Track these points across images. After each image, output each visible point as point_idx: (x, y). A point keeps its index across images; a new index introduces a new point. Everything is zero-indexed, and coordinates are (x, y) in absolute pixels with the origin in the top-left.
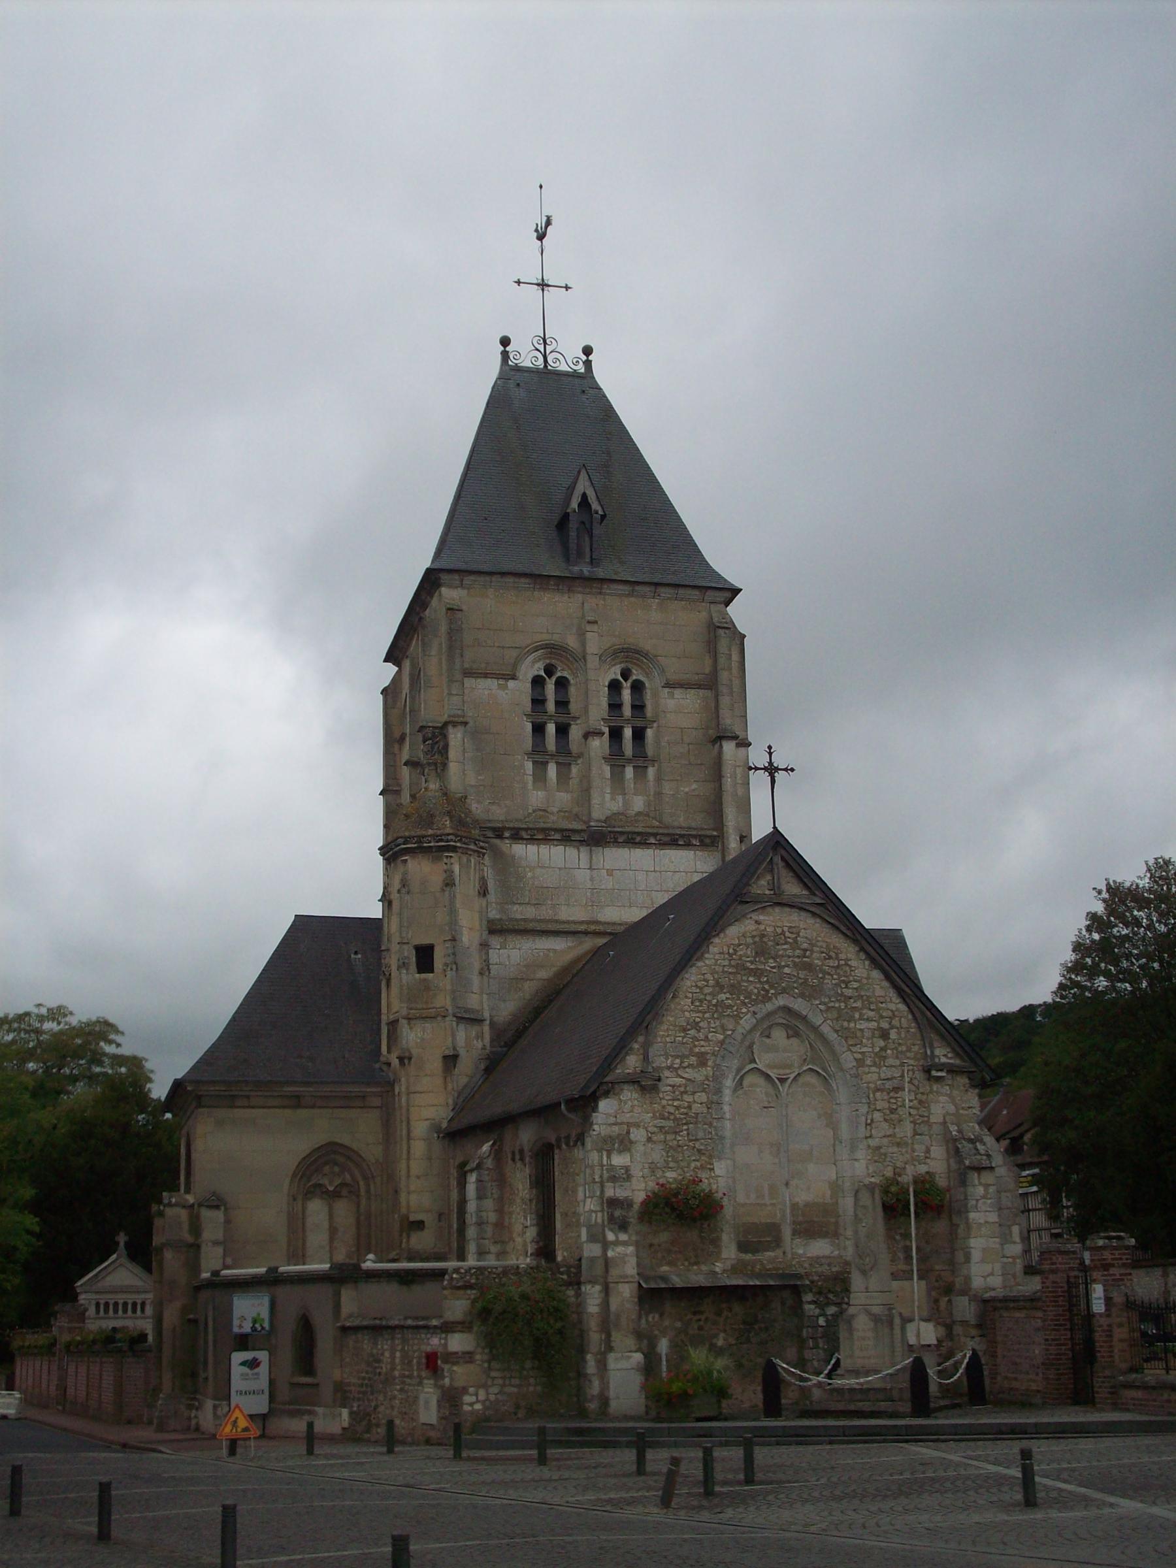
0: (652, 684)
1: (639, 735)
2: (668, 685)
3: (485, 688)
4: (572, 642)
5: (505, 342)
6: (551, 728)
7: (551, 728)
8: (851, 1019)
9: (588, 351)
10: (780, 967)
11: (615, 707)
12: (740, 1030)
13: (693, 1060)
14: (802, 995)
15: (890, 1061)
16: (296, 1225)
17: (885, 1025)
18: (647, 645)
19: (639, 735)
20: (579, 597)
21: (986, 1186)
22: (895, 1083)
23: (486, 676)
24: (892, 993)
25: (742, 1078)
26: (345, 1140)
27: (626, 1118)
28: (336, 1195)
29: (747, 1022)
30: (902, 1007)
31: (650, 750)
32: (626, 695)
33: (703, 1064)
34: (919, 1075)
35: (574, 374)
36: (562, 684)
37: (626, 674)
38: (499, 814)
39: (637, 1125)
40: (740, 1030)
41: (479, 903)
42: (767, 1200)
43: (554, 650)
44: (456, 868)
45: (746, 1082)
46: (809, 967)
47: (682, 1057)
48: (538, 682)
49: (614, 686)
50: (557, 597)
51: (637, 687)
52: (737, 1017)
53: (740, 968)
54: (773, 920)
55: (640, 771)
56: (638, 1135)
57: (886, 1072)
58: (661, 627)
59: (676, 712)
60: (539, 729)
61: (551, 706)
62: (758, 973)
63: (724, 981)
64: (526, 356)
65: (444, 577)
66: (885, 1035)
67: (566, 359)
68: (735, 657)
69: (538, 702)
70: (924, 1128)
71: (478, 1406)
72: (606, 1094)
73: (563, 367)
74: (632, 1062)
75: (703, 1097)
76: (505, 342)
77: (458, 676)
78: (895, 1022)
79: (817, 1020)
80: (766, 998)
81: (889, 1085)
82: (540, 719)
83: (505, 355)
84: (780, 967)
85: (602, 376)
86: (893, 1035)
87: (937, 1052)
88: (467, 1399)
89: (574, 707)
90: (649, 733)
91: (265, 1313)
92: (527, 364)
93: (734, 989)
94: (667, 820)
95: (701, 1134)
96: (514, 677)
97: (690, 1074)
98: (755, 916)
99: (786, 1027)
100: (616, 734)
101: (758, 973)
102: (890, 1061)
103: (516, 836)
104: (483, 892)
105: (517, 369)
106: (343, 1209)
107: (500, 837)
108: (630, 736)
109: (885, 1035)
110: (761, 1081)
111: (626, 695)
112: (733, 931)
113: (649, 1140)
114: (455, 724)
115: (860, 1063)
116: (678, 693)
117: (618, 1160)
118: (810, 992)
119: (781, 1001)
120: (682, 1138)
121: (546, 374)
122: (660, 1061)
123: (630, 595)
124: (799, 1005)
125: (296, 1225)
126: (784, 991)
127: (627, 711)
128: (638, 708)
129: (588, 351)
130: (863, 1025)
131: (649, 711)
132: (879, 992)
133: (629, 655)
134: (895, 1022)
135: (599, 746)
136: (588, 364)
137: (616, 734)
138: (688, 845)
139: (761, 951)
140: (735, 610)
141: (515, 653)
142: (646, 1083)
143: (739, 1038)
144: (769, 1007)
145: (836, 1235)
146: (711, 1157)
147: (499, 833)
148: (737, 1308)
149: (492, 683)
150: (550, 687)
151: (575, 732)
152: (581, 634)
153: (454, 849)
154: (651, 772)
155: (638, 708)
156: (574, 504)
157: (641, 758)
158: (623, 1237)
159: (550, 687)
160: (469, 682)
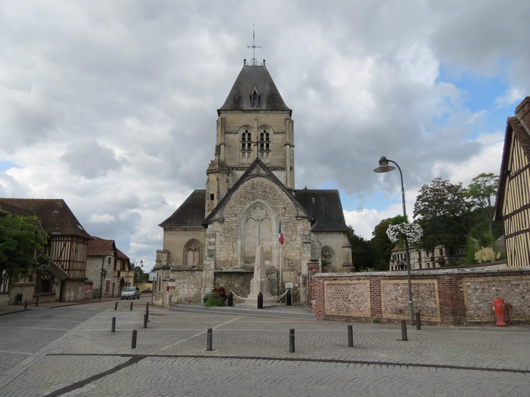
0: (271, 133)
2: (274, 133)
3: (231, 136)
4: (251, 124)
5: (245, 60)
6: (246, 145)
7: (246, 145)
8: (276, 205)
9: (264, 61)
10: (258, 192)
12: (246, 208)
13: (233, 215)
14: (263, 199)
15: (287, 215)
16: (185, 257)
17: (285, 206)
18: (270, 124)
19: (268, 145)
20: (253, 115)
21: (308, 247)
22: (288, 221)
23: (231, 133)
24: (288, 198)
25: (248, 220)
26: (196, 238)
27: (215, 229)
28: (195, 250)
29: (248, 206)
30: (291, 202)
31: (270, 148)
32: (265, 136)
33: (236, 216)
34: (294, 219)
35: (261, 66)
36: (249, 135)
37: (265, 132)
38: (233, 164)
39: (218, 231)
40: (246, 208)
41: (226, 184)
42: (253, 250)
43: (246, 126)
44: (220, 176)
45: (249, 221)
46: (265, 192)
47: (230, 215)
48: (244, 134)
50: (248, 115)
51: (268, 134)
52: (245, 205)
53: (247, 192)
54: (256, 180)
55: (268, 153)
56: (218, 234)
57: (285, 218)
58: (273, 120)
59: (275, 139)
60: (244, 145)
61: (247, 140)
62: (252, 193)
63: (243, 195)
64: (249, 63)
65: (221, 112)
66: (285, 208)
67: (259, 63)
68: (291, 126)
69: (244, 139)
70: (295, 232)
71: (176, 300)
72: (210, 224)
73: (258, 65)
74: (217, 216)
75: (236, 224)
76: (245, 60)
77: (223, 133)
78: (288, 205)
79: (267, 205)
80: (254, 199)
81: (286, 221)
82: (244, 142)
83: (245, 63)
84: (258, 192)
86: (288, 208)
87: (299, 213)
88: (173, 298)
91: (156, 277)
92: (250, 65)
93: (245, 198)
94: (273, 164)
95: (234, 234)
96: (237, 133)
97: (233, 219)
98: (252, 179)
99: (260, 207)
101: (252, 193)
102: (287, 215)
103: (237, 169)
104: (227, 182)
105: (247, 66)
106: (196, 253)
107: (233, 169)
109: (285, 208)
110: (253, 220)
111: (265, 136)
112: (246, 183)
113: (221, 235)
114: (222, 144)
115: (278, 216)
116: (277, 135)
117: (212, 240)
118: (265, 198)
119: (257, 200)
120: (229, 235)
121: (255, 67)
122: (225, 216)
123: (266, 113)
124: (262, 201)
125: (185, 257)
126: (258, 198)
127: (265, 140)
129: (264, 61)
130: (280, 206)
131: (270, 140)
132: (284, 198)
134: (288, 205)
136: (264, 63)
138: (278, 170)
139: (253, 188)
141: (238, 128)
142: (222, 221)
143: (246, 209)
144: (254, 202)
145: (271, 260)
146: (237, 239)
147: (233, 168)
148: (242, 278)
149: (232, 135)
150: (246, 135)
152: (253, 123)
153: (219, 172)
154: (270, 153)
155: (268, 139)
156: (252, 93)
157: (268, 150)
158: (211, 259)
159: (246, 135)
160: (226, 135)
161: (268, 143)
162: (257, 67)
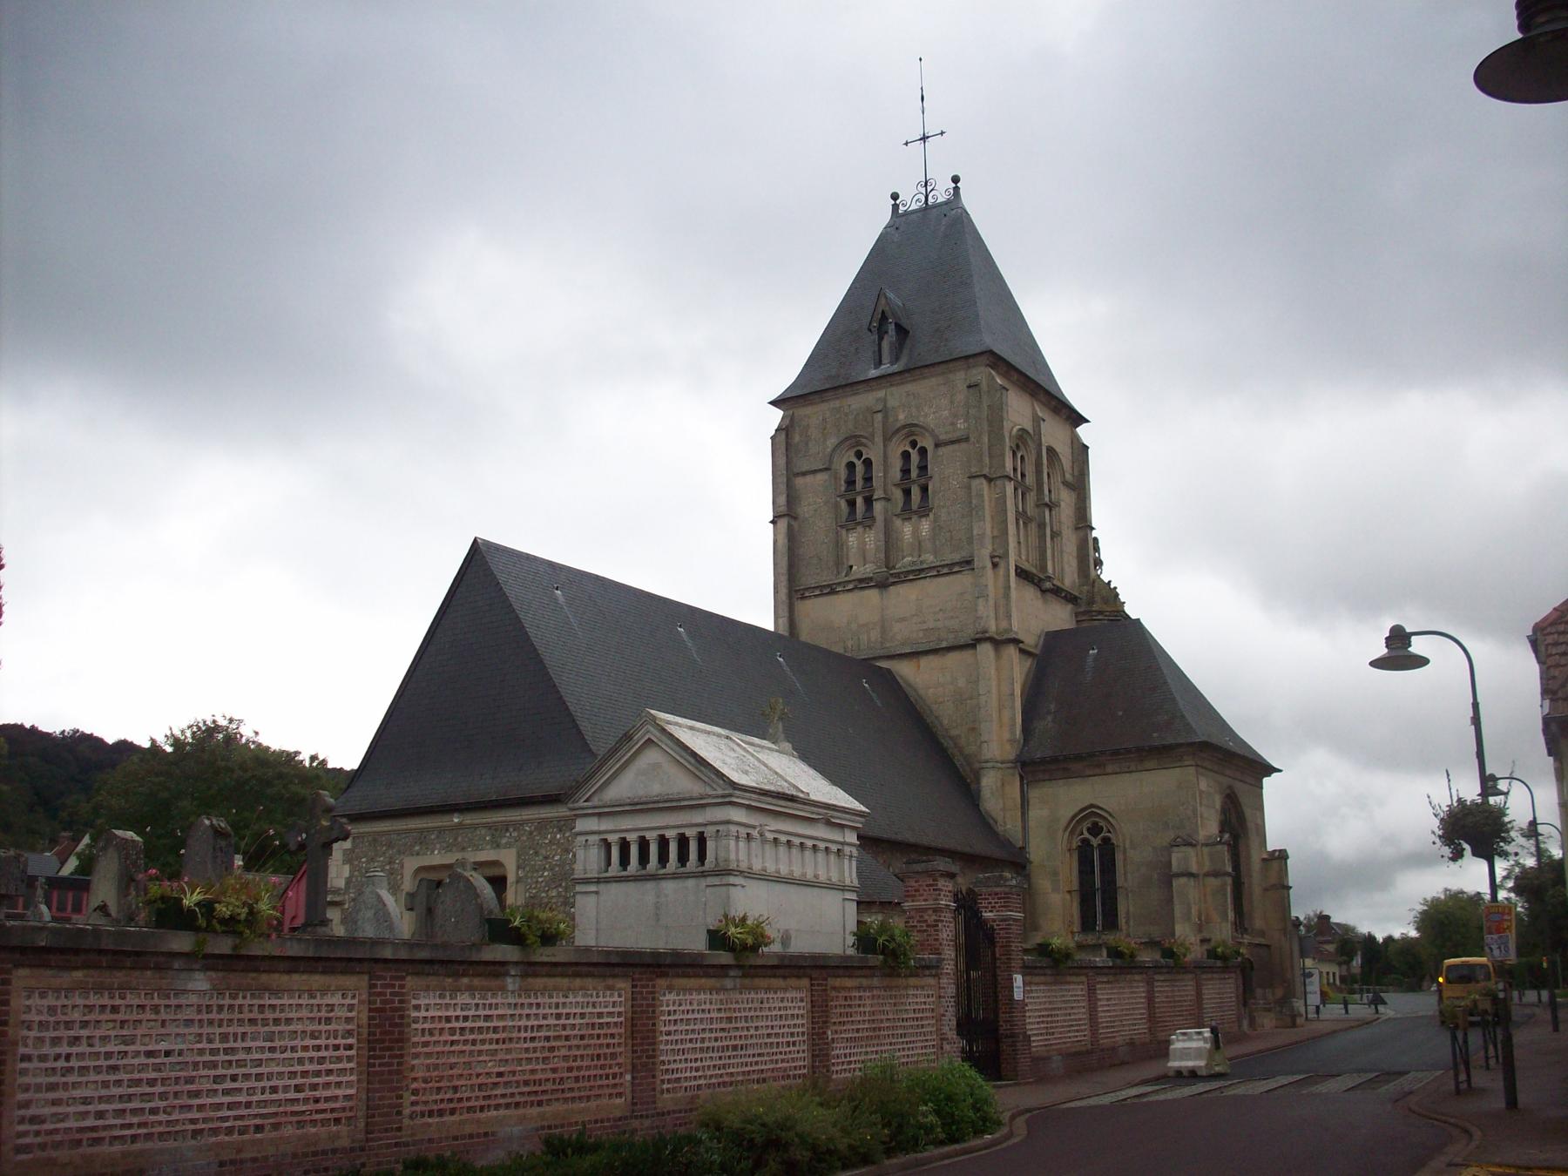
5: (895, 197)
7: (859, 501)
9: (956, 180)
11: (906, 471)
32: (915, 457)
49: (906, 456)
51: (923, 451)
64: (911, 200)
67: (941, 194)
76: (895, 197)
83: (895, 207)
92: (914, 207)
108: (916, 490)
111: (915, 457)
129: (956, 180)
133: (911, 431)
136: (956, 189)
155: (923, 468)
161: (923, 481)
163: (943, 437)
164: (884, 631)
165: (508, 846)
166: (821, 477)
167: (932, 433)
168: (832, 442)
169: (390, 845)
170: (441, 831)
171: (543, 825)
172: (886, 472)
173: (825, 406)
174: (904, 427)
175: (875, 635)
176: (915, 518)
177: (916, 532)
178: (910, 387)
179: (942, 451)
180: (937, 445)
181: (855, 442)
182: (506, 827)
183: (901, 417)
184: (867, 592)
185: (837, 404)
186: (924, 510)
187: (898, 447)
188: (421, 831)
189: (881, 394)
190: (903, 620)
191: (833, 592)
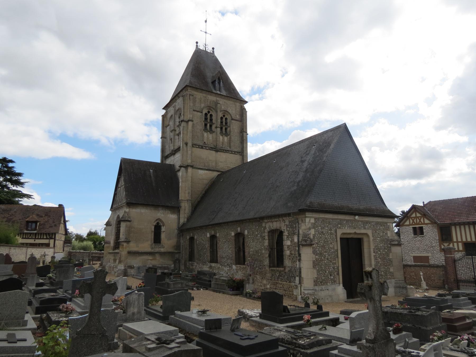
1: (226, 129)
5: (197, 43)
6: (208, 125)
9: (213, 49)
11: (222, 122)
19: (226, 129)
49: (222, 118)
51: (226, 119)
60: (206, 125)
64: (202, 47)
67: (209, 50)
69: (206, 119)
76: (197, 43)
82: (206, 123)
83: (197, 46)
85: (216, 54)
89: (214, 121)
90: (228, 129)
92: (201, 49)
100: (221, 128)
121: (206, 52)
128: (226, 123)
129: (213, 49)
133: (225, 112)
135: (219, 129)
136: (213, 51)
137: (221, 128)
140: (246, 106)
151: (213, 127)
155: (226, 123)
161: (226, 127)
162: (207, 52)
163: (233, 118)
164: (216, 163)
165: (368, 229)
166: (199, 114)
167: (230, 115)
168: (203, 105)
169: (329, 223)
170: (347, 221)
171: (377, 223)
172: (217, 121)
173: (201, 94)
174: (224, 111)
175: (214, 164)
176: (224, 136)
177: (223, 139)
178: (225, 100)
179: (233, 121)
180: (232, 119)
181: (210, 108)
182: (367, 222)
183: (223, 107)
184: (212, 151)
185: (205, 95)
186: (226, 134)
187: (220, 115)
188: (341, 220)
189: (218, 99)
190: (221, 162)
191: (202, 148)
